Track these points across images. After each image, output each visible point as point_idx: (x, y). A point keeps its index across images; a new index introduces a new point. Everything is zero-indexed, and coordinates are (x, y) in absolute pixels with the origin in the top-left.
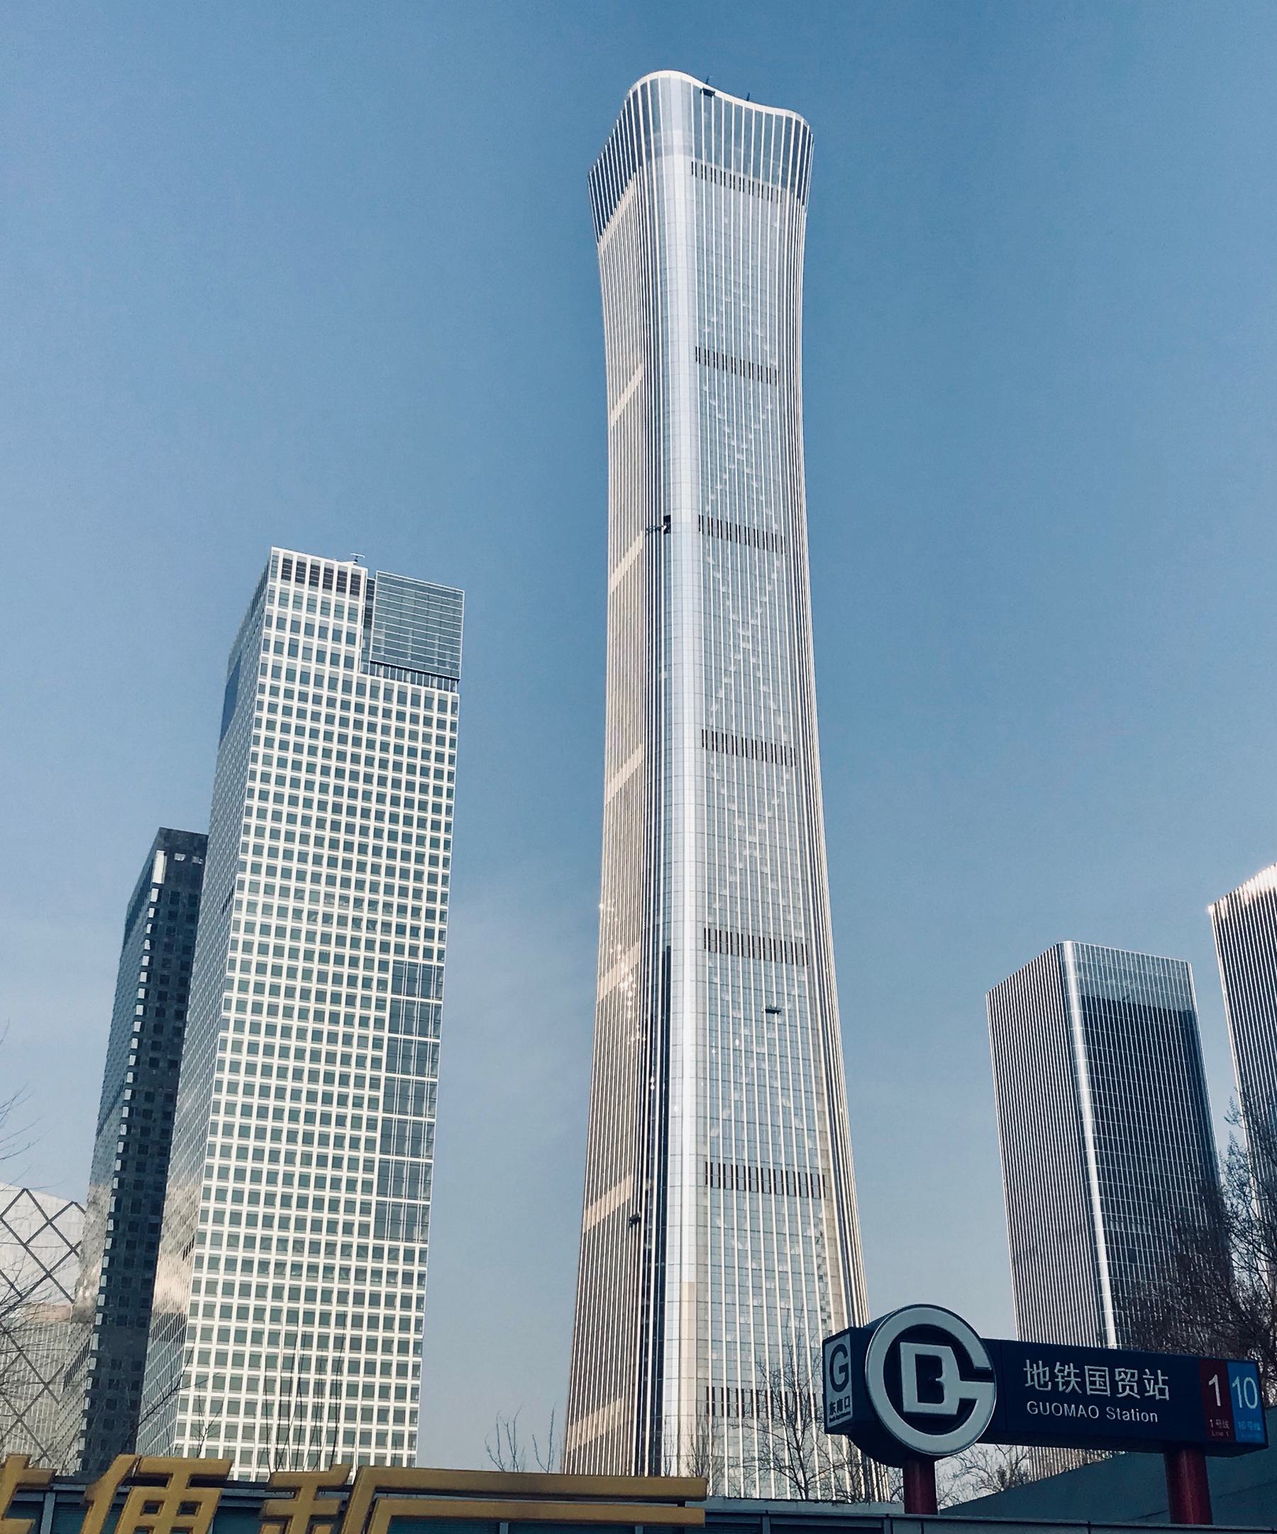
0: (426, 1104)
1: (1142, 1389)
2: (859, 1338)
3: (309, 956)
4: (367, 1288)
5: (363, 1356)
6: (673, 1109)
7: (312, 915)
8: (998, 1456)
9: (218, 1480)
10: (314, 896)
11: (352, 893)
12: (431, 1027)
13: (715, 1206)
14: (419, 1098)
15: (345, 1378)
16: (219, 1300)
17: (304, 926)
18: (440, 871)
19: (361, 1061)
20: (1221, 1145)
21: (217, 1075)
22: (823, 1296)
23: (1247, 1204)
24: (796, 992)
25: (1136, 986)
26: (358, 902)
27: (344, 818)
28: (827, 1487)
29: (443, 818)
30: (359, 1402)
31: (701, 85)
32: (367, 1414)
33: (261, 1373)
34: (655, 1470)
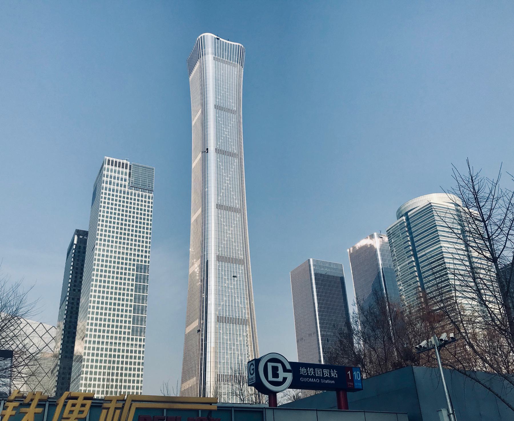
0: (145, 301)
1: (330, 375)
2: (257, 361)
3: (114, 262)
4: (130, 348)
5: (128, 366)
6: (209, 302)
7: (115, 252)
8: (293, 392)
9: (91, 398)
10: (116, 247)
11: (126, 246)
12: (146, 281)
13: (220, 327)
14: (143, 299)
15: (124, 372)
16: (91, 351)
17: (113, 255)
18: (148, 240)
19: (128, 290)
20: (351, 311)
21: (90, 293)
22: (248, 351)
23: (358, 327)
24: (241, 272)
25: (329, 270)
26: (127, 249)
27: (123, 227)
28: (249, 400)
29: (149, 227)
30: (127, 378)
31: (216, 37)
32: (129, 381)
33: (102, 371)
34: (204, 396)
